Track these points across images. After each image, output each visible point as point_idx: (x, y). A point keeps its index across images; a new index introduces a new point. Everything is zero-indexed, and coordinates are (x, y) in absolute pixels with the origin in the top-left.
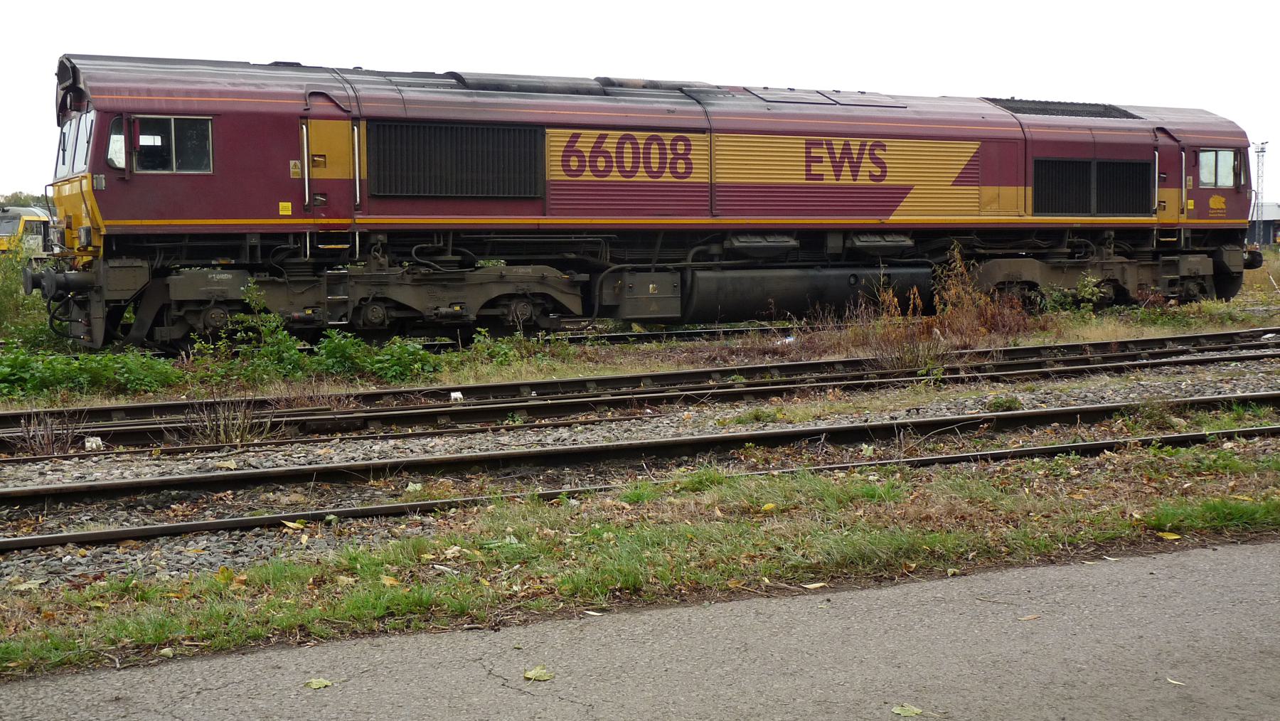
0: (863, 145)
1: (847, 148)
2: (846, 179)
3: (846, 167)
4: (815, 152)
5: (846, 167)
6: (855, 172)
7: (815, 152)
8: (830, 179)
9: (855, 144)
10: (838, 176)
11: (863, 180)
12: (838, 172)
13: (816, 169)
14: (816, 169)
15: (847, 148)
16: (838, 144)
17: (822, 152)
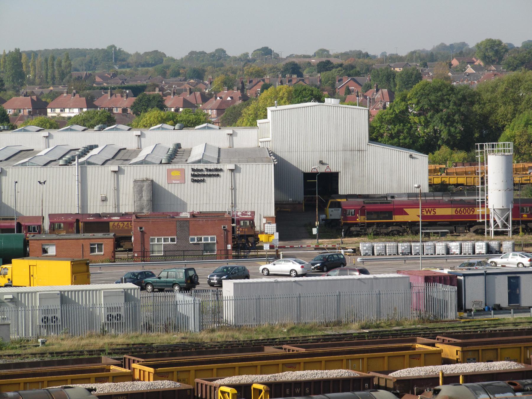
0: (431, 209)
1: (429, 210)
2: (429, 214)
3: (429, 212)
4: (423, 210)
5: (429, 212)
6: (430, 213)
7: (423, 210)
8: (425, 214)
9: (430, 209)
10: (427, 213)
11: (432, 214)
12: (427, 213)
13: (423, 213)
14: (423, 213)
15: (429, 210)
16: (427, 209)
17: (424, 210)
